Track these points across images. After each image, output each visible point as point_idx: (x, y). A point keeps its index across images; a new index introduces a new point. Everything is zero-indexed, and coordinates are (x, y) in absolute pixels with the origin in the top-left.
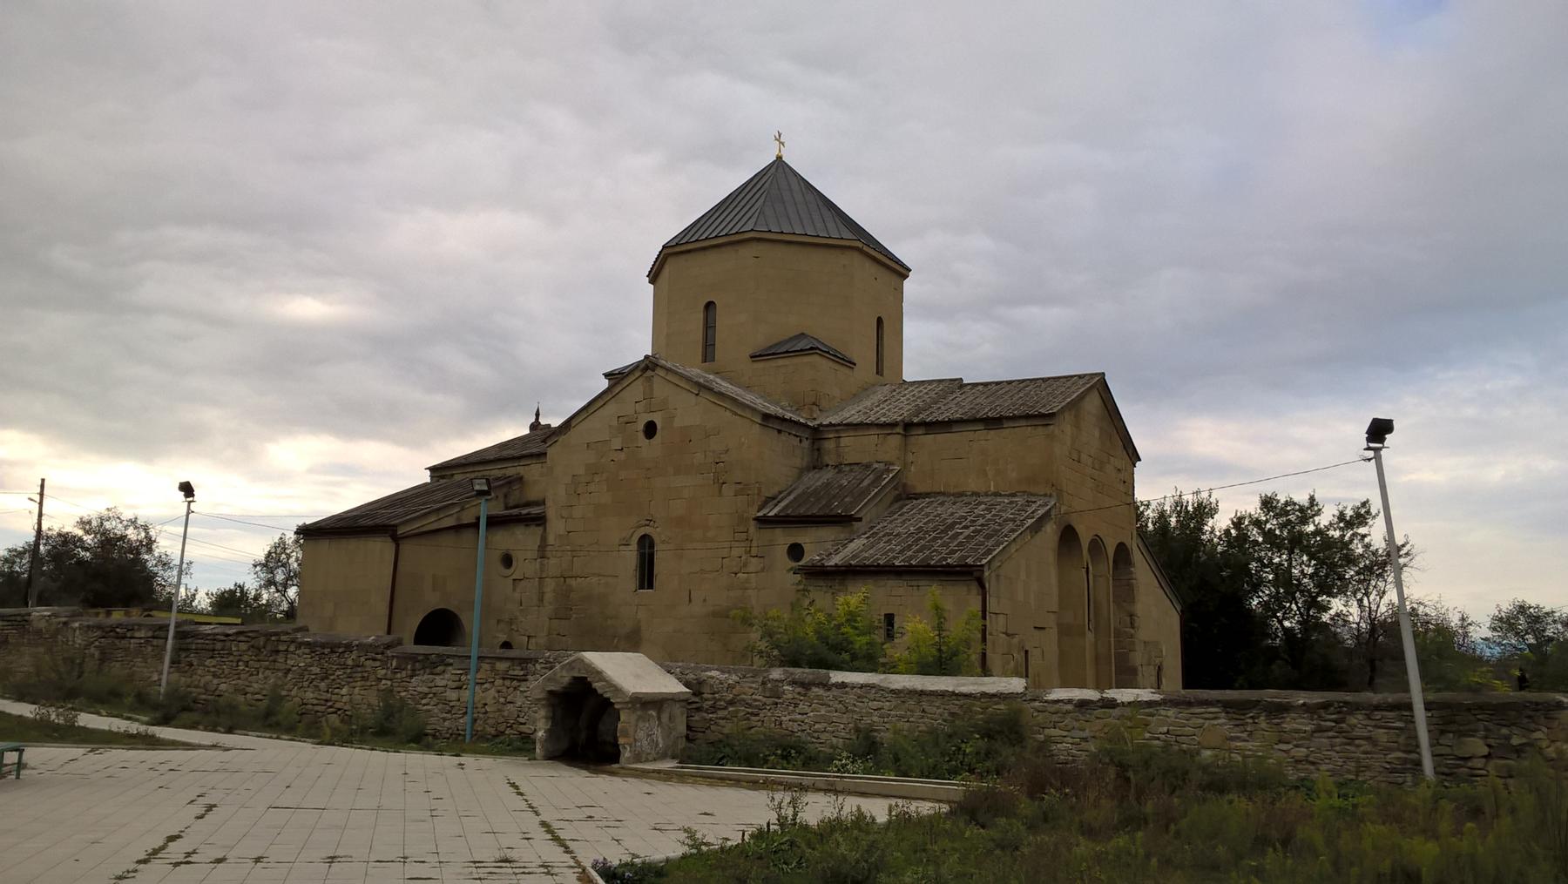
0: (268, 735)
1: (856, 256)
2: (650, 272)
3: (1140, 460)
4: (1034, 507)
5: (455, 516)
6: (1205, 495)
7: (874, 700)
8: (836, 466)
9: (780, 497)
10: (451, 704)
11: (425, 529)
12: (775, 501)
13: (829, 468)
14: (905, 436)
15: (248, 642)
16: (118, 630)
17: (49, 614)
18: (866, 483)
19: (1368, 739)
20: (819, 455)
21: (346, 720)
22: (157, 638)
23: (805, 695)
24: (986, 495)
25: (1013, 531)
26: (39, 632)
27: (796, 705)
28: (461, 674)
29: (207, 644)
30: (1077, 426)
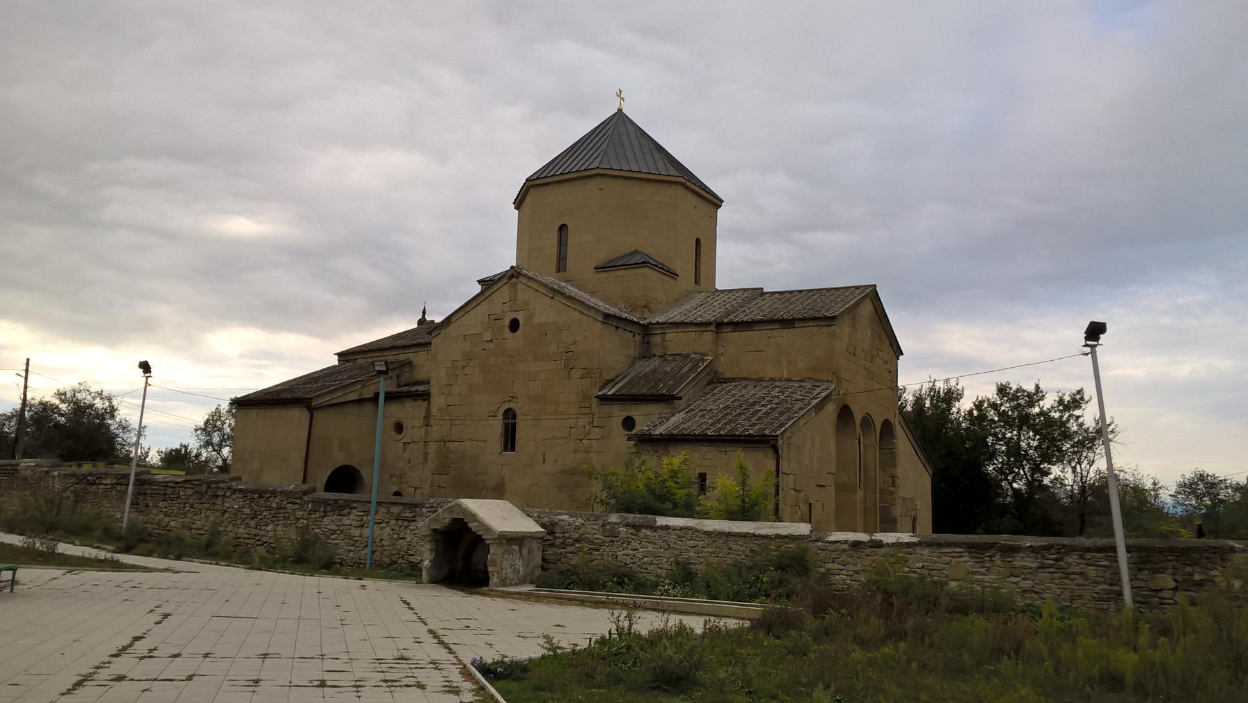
0: (209, 562)
1: (681, 190)
2: (515, 200)
3: (902, 354)
4: (819, 390)
5: (357, 392)
6: (953, 383)
7: (691, 540)
8: (662, 356)
9: (617, 380)
10: (355, 539)
11: (331, 402)
12: (613, 384)
13: (656, 357)
14: (717, 332)
15: (193, 488)
16: (89, 478)
18: (685, 369)
19: (1081, 574)
21: (271, 550)
22: (120, 484)
23: (636, 535)
25: (801, 409)
26: (26, 479)
27: (629, 543)
28: (363, 516)
29: (161, 490)
30: (854, 326)
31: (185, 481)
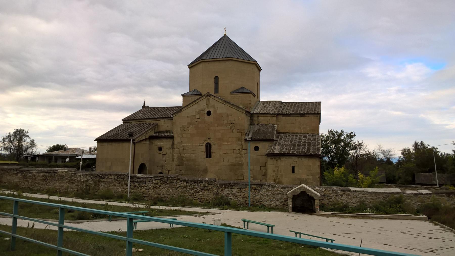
0: (200, 207)
8: (258, 125)
10: (238, 197)
12: (247, 135)
16: (101, 176)
17: (67, 171)
20: (252, 121)
22: (119, 178)
23: (344, 193)
24: (301, 133)
26: (63, 176)
27: (342, 196)
28: (241, 189)
29: (143, 180)
31: (154, 177)
